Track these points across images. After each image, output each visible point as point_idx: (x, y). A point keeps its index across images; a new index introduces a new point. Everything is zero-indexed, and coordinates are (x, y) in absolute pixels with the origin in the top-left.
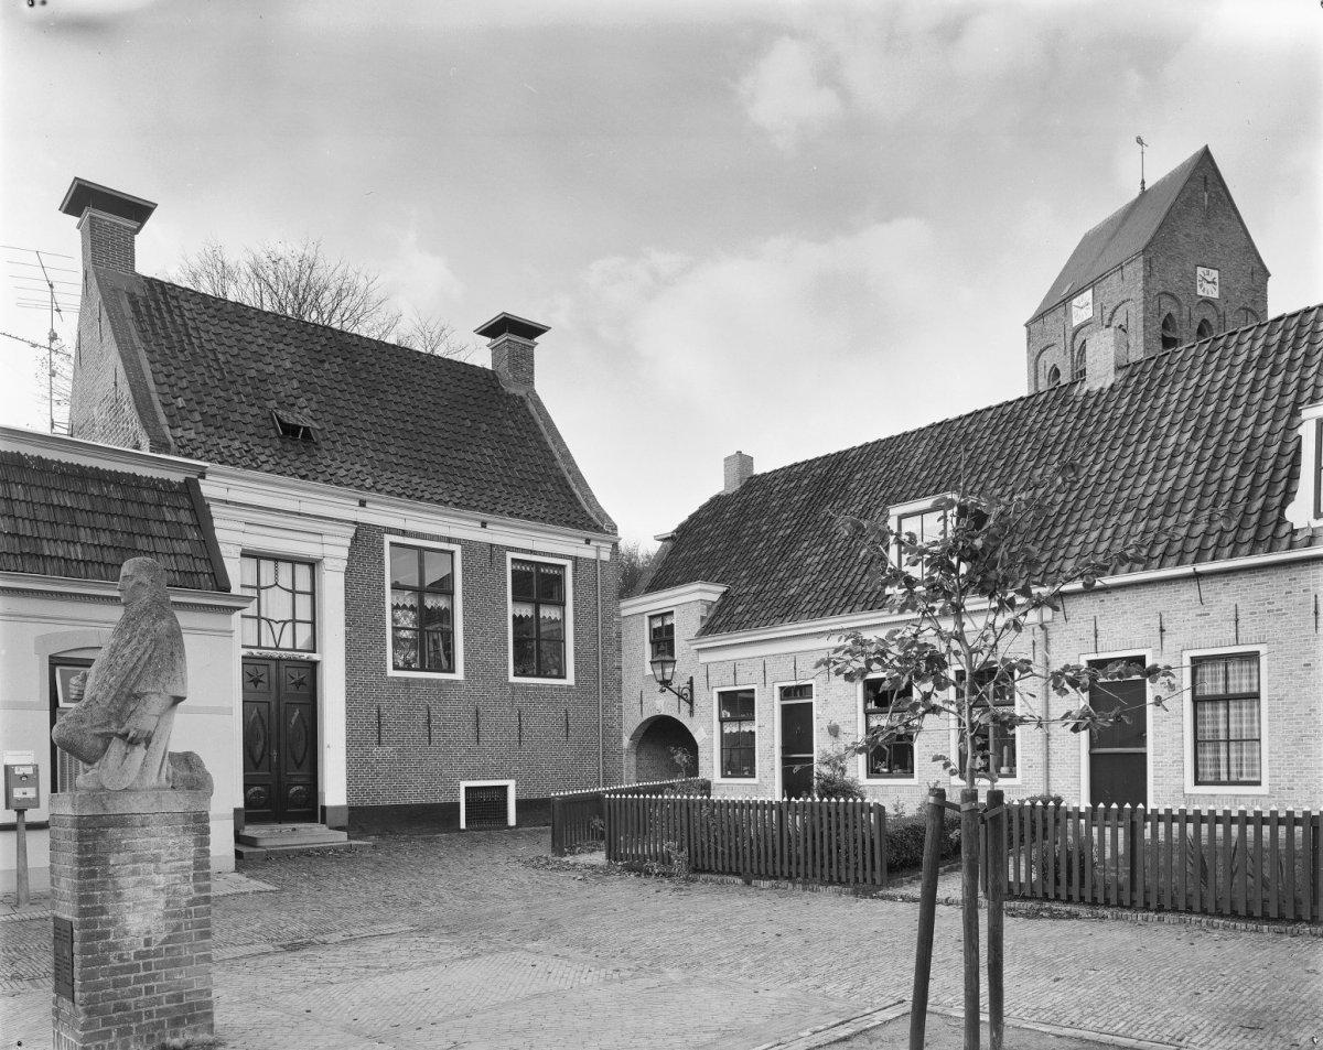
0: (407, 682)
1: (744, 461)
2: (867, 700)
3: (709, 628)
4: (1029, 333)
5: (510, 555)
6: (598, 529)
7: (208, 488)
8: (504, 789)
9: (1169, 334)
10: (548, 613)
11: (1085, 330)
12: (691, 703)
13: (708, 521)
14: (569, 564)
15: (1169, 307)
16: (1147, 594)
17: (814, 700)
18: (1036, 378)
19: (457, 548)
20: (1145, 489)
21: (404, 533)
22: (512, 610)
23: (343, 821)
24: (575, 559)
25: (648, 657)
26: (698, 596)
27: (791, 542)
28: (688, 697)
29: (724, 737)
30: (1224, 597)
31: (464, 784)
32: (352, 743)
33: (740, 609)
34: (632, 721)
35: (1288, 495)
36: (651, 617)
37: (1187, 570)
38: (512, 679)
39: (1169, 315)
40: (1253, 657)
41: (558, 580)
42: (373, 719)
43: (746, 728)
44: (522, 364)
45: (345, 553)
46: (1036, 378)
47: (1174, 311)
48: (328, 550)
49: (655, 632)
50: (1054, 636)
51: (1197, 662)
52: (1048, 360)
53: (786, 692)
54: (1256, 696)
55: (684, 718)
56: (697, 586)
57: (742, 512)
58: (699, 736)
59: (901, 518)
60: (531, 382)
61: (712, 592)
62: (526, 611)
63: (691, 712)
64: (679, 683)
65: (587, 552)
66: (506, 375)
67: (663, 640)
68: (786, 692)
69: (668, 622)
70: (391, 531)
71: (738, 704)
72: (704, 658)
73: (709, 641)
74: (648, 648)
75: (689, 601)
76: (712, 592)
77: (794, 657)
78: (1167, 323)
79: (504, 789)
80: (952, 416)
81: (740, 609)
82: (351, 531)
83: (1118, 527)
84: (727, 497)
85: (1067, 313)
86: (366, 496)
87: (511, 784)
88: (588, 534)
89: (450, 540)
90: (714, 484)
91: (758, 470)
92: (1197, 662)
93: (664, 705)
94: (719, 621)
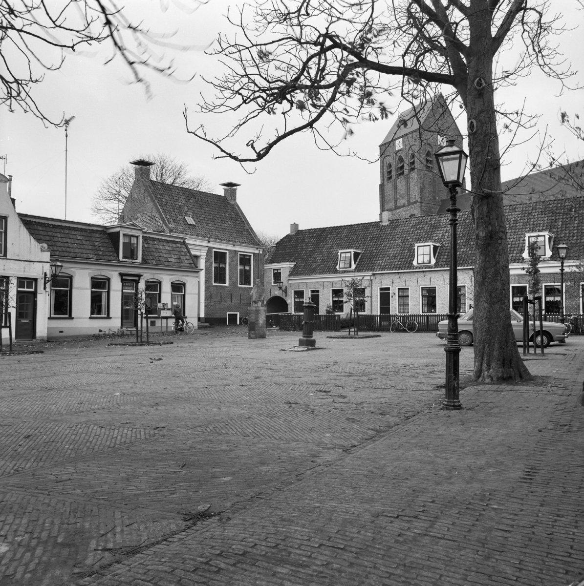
0: (217, 287)
1: (295, 226)
2: (333, 294)
3: (292, 274)
4: (380, 149)
5: (239, 253)
6: (259, 245)
7: (187, 241)
8: (237, 314)
9: (429, 158)
10: (247, 268)
11: (400, 152)
12: (286, 293)
13: (287, 242)
14: (252, 255)
15: (428, 149)
16: (390, 275)
17: (320, 294)
18: (383, 166)
19: (227, 252)
20: (392, 252)
21: (217, 248)
22: (239, 267)
23: (204, 321)
24: (254, 253)
25: (273, 281)
26: (289, 266)
27: (312, 252)
28: (285, 291)
29: (295, 302)
30: (404, 277)
31: (228, 313)
32: (206, 301)
33: (300, 270)
34: (267, 297)
35: (413, 260)
36: (274, 270)
37: (397, 271)
38: (239, 286)
39: (429, 152)
40: (408, 289)
41: (249, 260)
42: (219, 297)
43: (302, 300)
44: (233, 194)
45: (205, 254)
46: (383, 166)
47: (430, 150)
48: (202, 254)
49: (274, 274)
50: (373, 282)
51: (399, 289)
52: (389, 160)
53: (312, 291)
54: (408, 296)
55: (284, 297)
56: (288, 263)
57: (297, 241)
58: (288, 301)
59: (341, 253)
60: (235, 200)
61: (292, 265)
62: (242, 268)
63: (286, 296)
64: (283, 288)
65: (257, 252)
66: (229, 198)
67: (277, 276)
68: (312, 291)
69: (279, 271)
70: (214, 248)
71: (299, 294)
72: (290, 282)
73: (292, 278)
74: (272, 278)
75: (285, 267)
76: (292, 265)
77: (315, 283)
78: (428, 154)
79: (237, 314)
80: (353, 224)
81: (300, 270)
82: (207, 249)
83: (386, 260)
84: (291, 235)
85: (394, 145)
86: (210, 239)
87: (238, 313)
88: (257, 247)
89: (226, 250)
90: (286, 231)
91: (300, 228)
92: (399, 289)
93: (277, 293)
94: (294, 273)
